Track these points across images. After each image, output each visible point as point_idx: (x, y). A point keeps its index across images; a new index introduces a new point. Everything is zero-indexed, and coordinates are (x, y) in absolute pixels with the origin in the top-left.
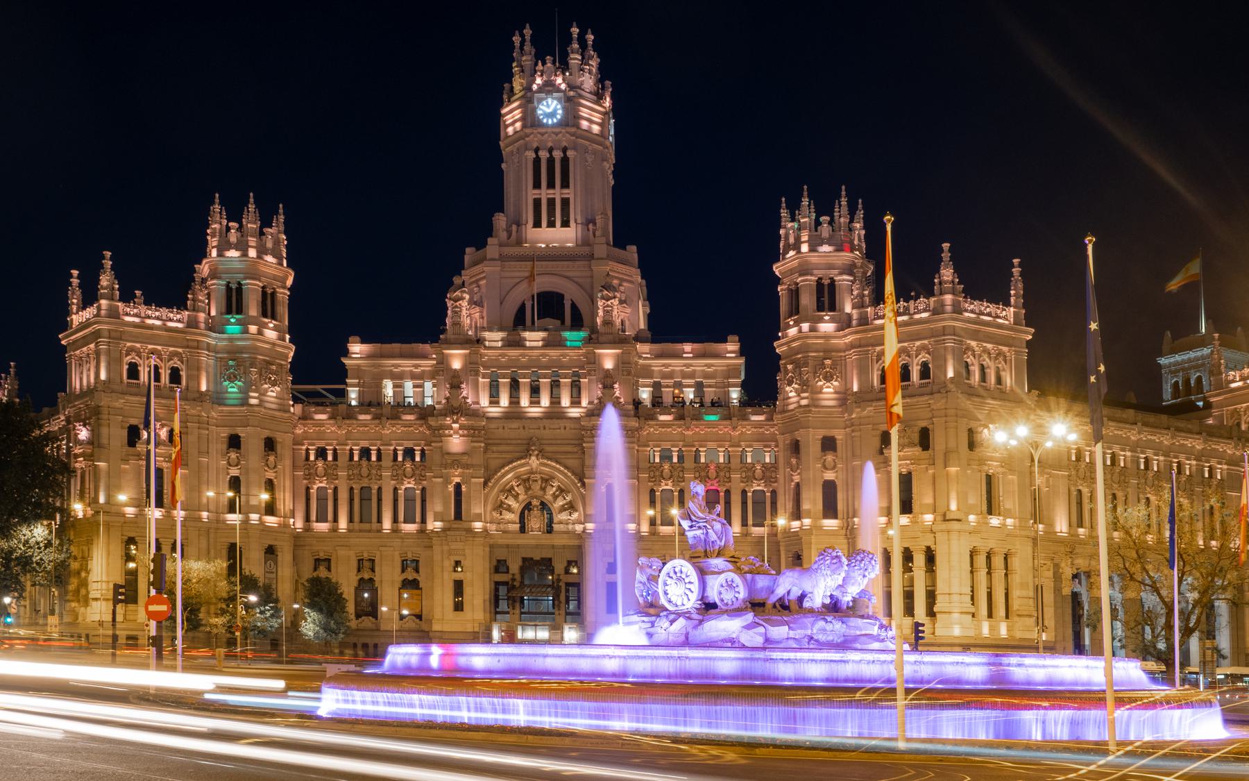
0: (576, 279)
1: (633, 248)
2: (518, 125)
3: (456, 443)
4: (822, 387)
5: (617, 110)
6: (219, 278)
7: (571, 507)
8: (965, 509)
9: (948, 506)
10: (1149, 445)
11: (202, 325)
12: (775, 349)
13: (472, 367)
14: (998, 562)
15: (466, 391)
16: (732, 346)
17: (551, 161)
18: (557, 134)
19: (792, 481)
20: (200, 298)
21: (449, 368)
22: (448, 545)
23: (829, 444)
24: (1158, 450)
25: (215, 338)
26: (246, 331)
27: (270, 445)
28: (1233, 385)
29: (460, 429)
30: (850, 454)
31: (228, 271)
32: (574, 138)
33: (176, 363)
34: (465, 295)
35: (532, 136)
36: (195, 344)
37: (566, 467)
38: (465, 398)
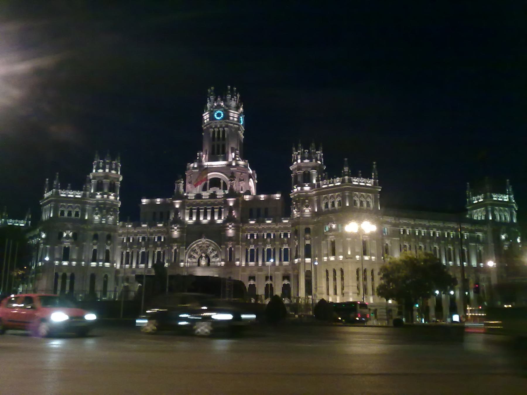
0: (226, 173)
1: (247, 161)
2: (208, 120)
3: (176, 234)
4: (305, 210)
5: (245, 113)
8: (354, 254)
10: (435, 227)
12: (290, 196)
13: (183, 206)
14: (369, 274)
15: (180, 215)
16: (278, 196)
17: (219, 132)
19: (295, 244)
20: (88, 187)
23: (308, 231)
24: (438, 228)
25: (92, 200)
26: (103, 197)
32: (227, 123)
33: (77, 210)
34: (182, 181)
35: (212, 124)
38: (180, 218)
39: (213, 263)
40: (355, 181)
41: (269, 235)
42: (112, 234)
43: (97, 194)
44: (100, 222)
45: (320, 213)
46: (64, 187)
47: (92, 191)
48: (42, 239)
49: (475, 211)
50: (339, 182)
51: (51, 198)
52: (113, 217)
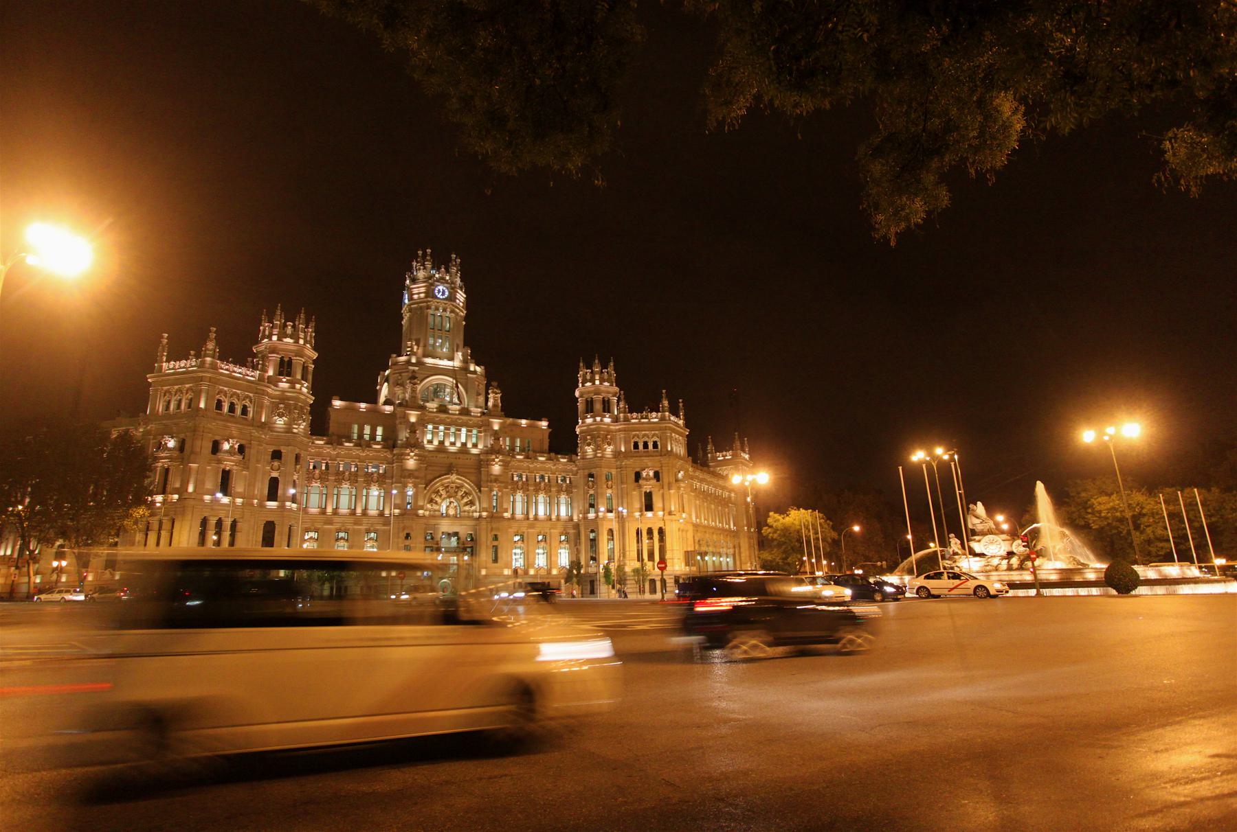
1: (483, 367)
2: (422, 295)
3: (411, 463)
4: (606, 449)
6: (278, 354)
7: (471, 503)
9: (670, 508)
11: (266, 381)
16: (544, 424)
18: (445, 304)
21: (408, 421)
22: (403, 523)
25: (273, 390)
26: (294, 387)
27: (297, 458)
28: (719, 459)
29: (415, 455)
30: (619, 482)
31: (283, 350)
36: (261, 392)
37: (471, 481)
38: (418, 439)
39: (466, 513)
40: (672, 418)
41: (542, 477)
42: (303, 454)
43: (281, 379)
44: (289, 430)
45: (627, 455)
46: (222, 359)
47: (271, 373)
48: (170, 449)
49: (718, 468)
50: (655, 418)
51: (201, 374)
52: (304, 424)
